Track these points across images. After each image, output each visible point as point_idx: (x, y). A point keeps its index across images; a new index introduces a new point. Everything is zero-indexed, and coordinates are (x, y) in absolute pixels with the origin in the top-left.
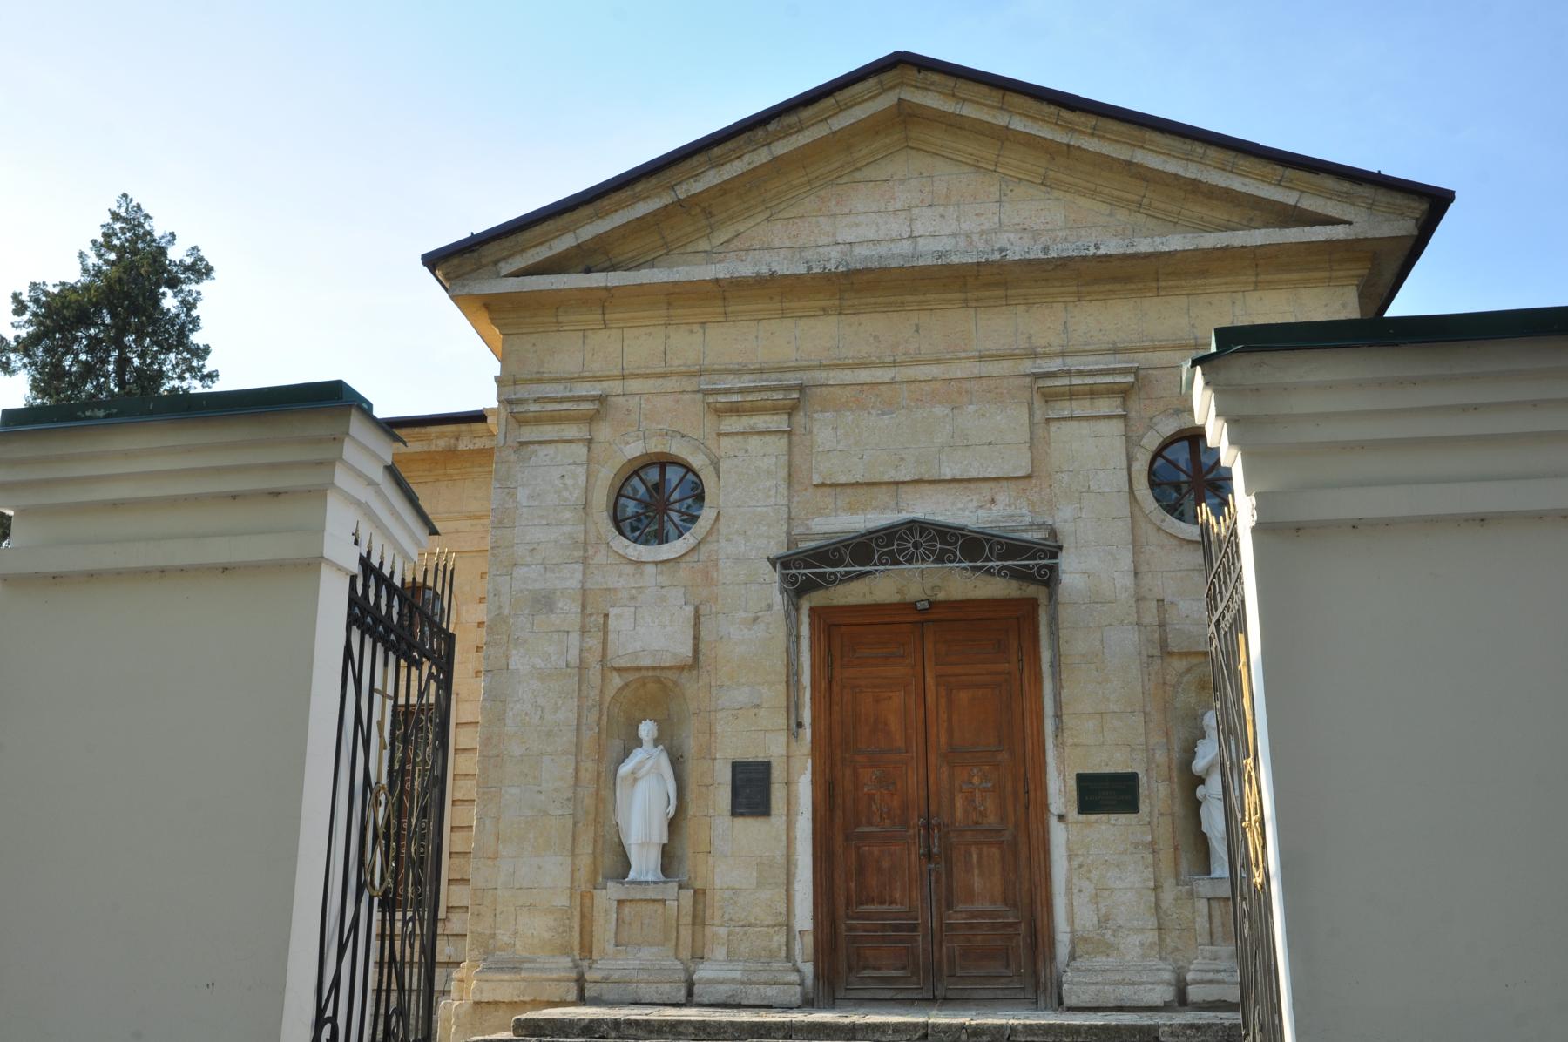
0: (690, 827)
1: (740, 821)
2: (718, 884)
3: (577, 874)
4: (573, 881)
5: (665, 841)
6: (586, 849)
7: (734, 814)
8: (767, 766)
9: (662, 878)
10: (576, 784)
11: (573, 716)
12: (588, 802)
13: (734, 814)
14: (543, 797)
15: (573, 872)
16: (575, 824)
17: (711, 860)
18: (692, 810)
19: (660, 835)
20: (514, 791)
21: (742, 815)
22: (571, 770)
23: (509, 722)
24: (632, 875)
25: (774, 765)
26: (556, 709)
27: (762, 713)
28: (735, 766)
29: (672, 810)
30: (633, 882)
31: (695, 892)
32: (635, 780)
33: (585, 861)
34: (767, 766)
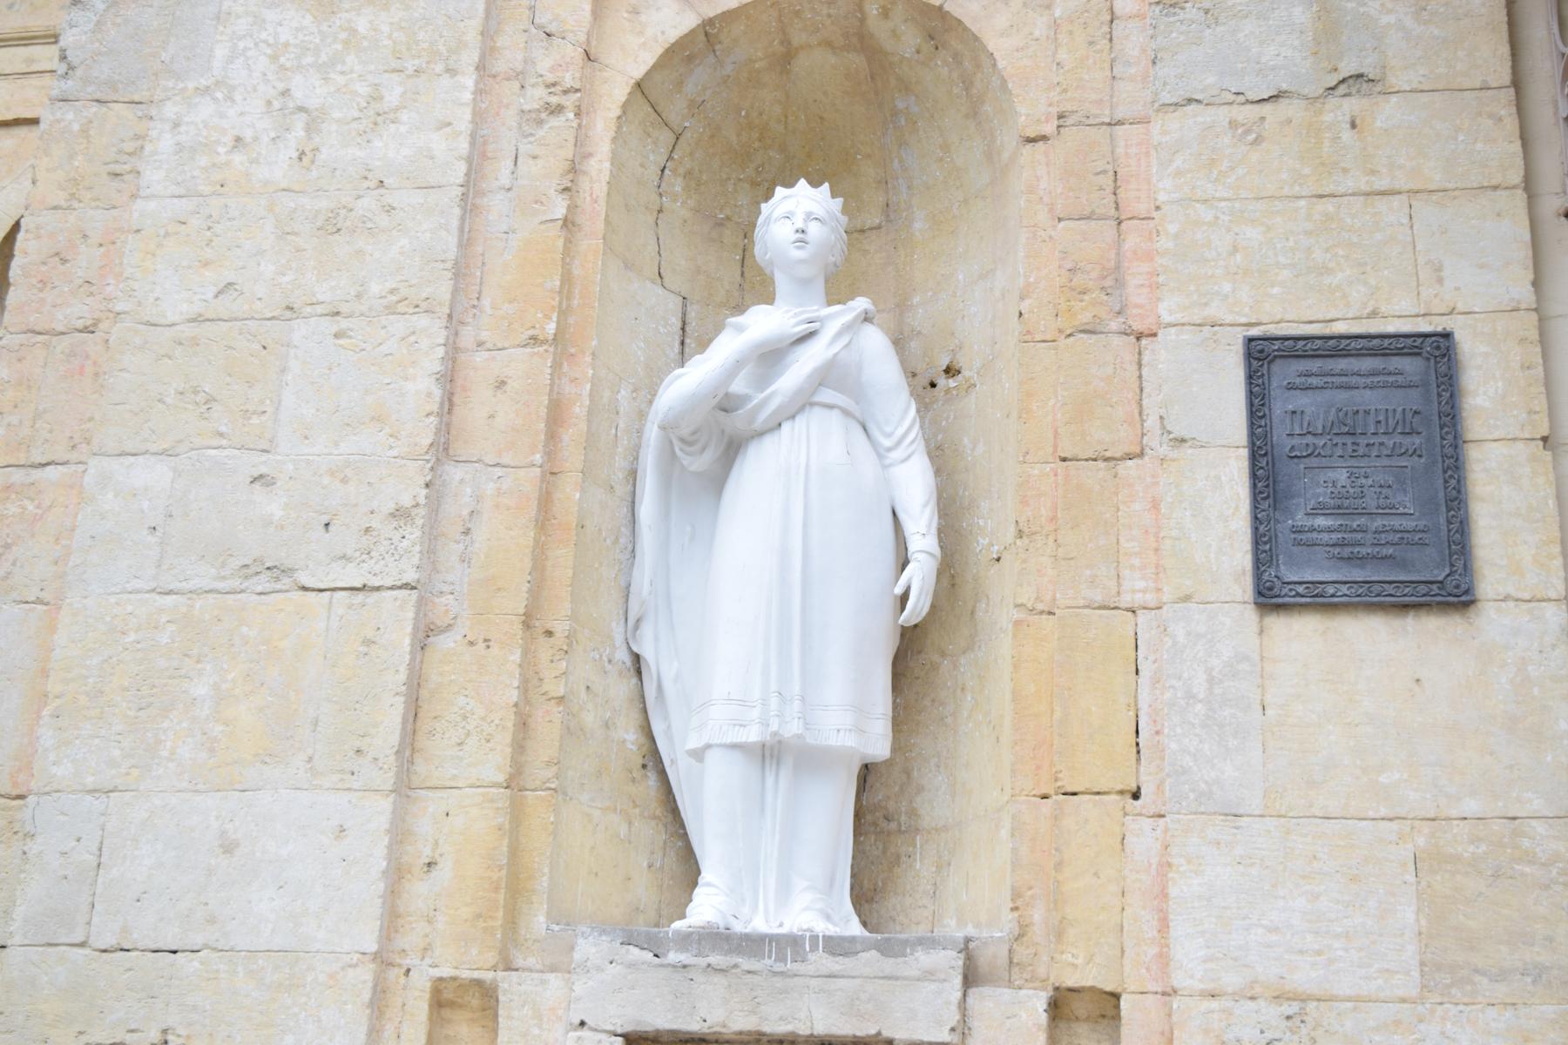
0: (998, 672)
1: (1301, 635)
2: (1191, 962)
3: (419, 892)
4: (392, 920)
5: (878, 746)
6: (469, 758)
7: (1270, 597)
8: (1436, 350)
9: (855, 928)
10: (443, 448)
11: (447, 154)
12: (502, 537)
13: (1270, 597)
14: (272, 505)
15: (396, 875)
16: (425, 635)
17: (1144, 838)
18: (1005, 594)
19: (850, 715)
20: (152, 475)
21: (1319, 601)
22: (422, 387)
23: (154, 176)
24: (706, 908)
25: (1472, 348)
26: (378, 117)
27: (1387, 113)
28: (1263, 355)
29: (920, 575)
30: (717, 938)
31: (1060, 1006)
32: (733, 449)
33: (460, 821)
34: (1436, 350)
